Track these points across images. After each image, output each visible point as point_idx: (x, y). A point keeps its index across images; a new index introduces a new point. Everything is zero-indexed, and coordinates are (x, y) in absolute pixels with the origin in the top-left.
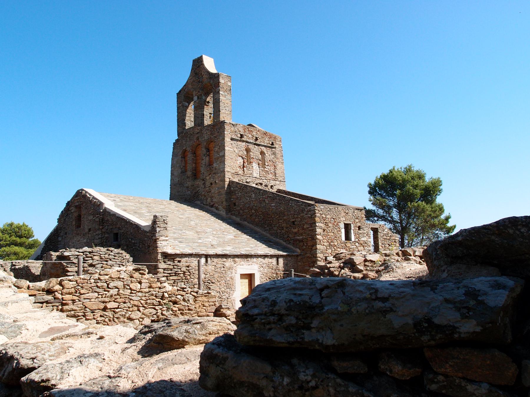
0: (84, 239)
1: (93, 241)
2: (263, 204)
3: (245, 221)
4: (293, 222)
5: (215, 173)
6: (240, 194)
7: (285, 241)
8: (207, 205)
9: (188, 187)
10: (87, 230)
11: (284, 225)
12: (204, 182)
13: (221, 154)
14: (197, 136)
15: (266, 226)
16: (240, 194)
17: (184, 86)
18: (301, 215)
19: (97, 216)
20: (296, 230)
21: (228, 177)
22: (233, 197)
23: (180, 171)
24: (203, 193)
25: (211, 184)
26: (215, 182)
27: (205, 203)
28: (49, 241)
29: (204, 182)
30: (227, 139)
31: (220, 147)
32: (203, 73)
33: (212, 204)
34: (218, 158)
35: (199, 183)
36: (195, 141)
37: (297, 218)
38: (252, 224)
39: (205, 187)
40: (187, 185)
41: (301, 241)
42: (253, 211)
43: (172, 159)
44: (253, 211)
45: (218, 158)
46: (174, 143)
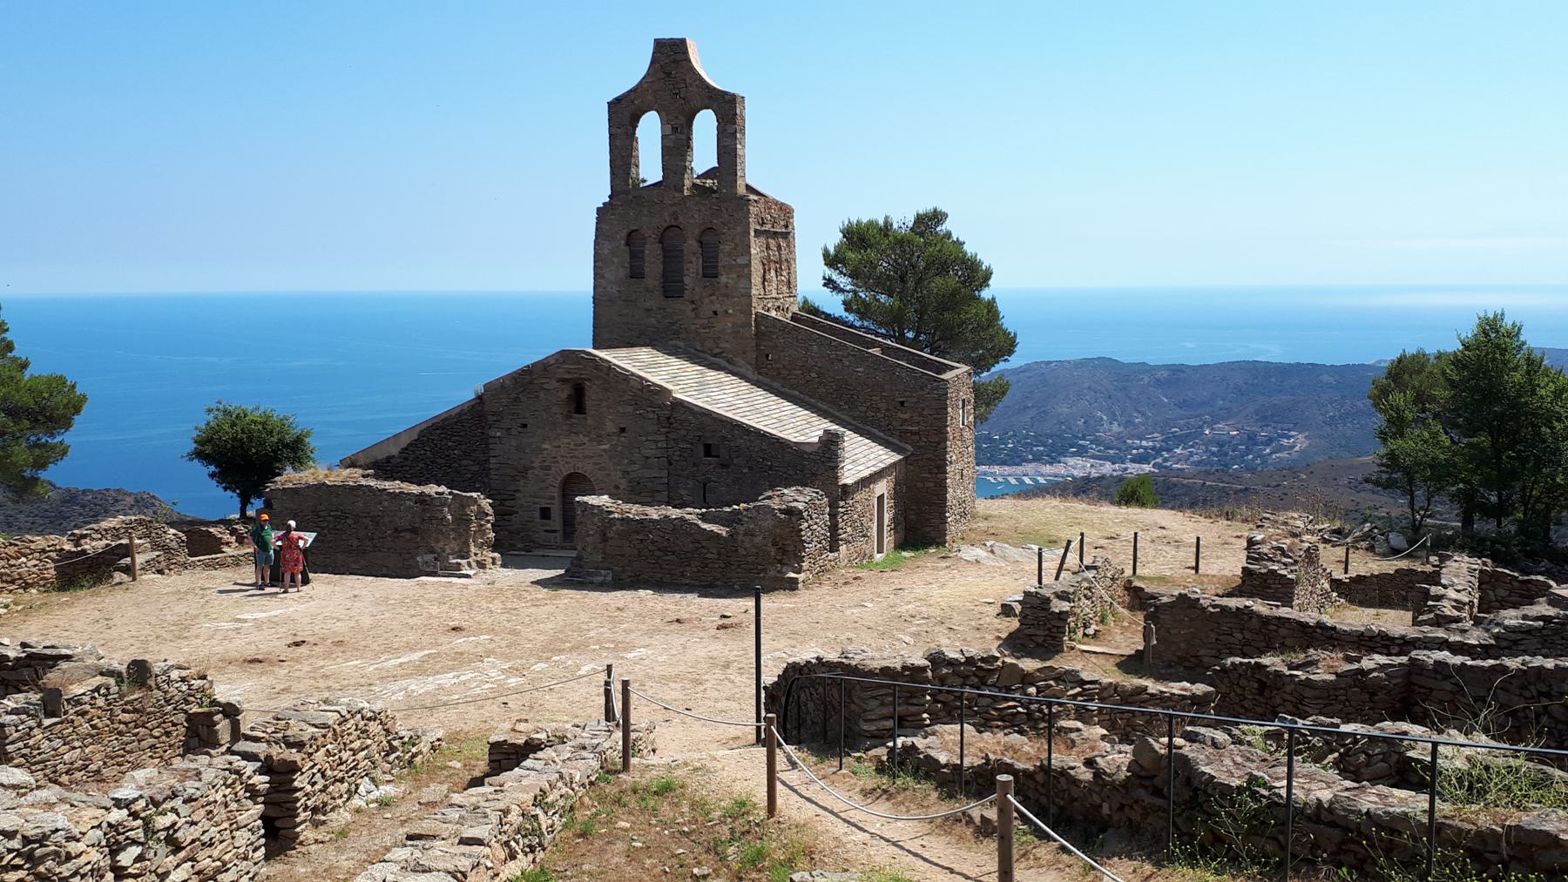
0: (599, 443)
1: (637, 450)
2: (838, 366)
3: (795, 389)
4: (902, 403)
5: (726, 296)
6: (782, 341)
7: (884, 431)
8: (704, 352)
9: (648, 310)
10: (611, 427)
11: (883, 405)
12: (694, 306)
13: (740, 261)
14: (674, 209)
15: (842, 403)
16: (782, 341)
17: (631, 91)
18: (921, 393)
19: (649, 409)
20: (906, 416)
21: (757, 308)
22: (765, 343)
23: (623, 273)
24: (693, 327)
25: (715, 313)
26: (726, 312)
27: (698, 348)
28: (438, 432)
29: (694, 306)
30: (752, 233)
31: (736, 245)
32: (688, 81)
33: (717, 351)
34: (731, 268)
35: (677, 305)
36: (667, 219)
37: (911, 397)
38: (811, 396)
39: (697, 316)
40: (647, 305)
41: (917, 433)
42: (813, 375)
43: (596, 243)
44: (813, 375)
45: (731, 268)
46: (599, 210)
